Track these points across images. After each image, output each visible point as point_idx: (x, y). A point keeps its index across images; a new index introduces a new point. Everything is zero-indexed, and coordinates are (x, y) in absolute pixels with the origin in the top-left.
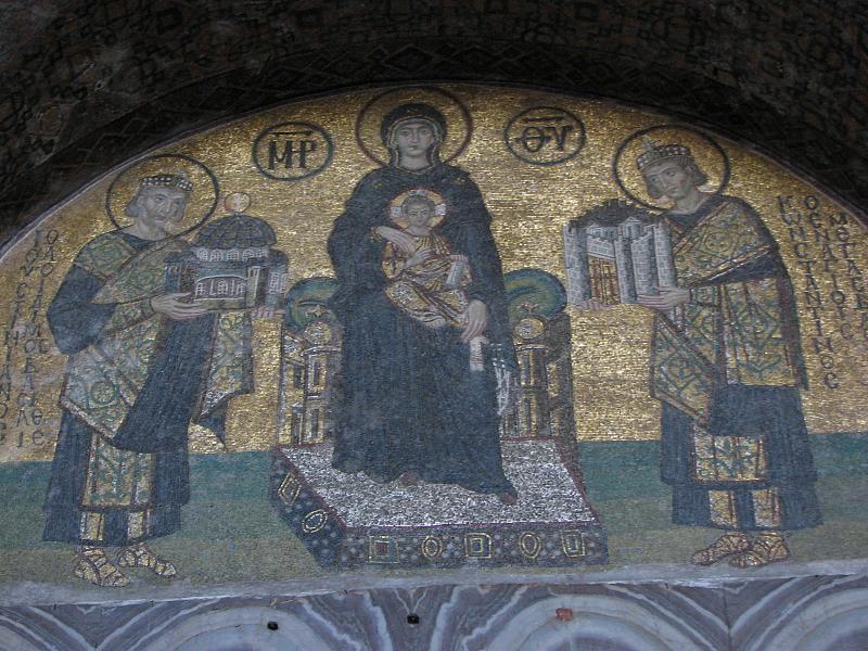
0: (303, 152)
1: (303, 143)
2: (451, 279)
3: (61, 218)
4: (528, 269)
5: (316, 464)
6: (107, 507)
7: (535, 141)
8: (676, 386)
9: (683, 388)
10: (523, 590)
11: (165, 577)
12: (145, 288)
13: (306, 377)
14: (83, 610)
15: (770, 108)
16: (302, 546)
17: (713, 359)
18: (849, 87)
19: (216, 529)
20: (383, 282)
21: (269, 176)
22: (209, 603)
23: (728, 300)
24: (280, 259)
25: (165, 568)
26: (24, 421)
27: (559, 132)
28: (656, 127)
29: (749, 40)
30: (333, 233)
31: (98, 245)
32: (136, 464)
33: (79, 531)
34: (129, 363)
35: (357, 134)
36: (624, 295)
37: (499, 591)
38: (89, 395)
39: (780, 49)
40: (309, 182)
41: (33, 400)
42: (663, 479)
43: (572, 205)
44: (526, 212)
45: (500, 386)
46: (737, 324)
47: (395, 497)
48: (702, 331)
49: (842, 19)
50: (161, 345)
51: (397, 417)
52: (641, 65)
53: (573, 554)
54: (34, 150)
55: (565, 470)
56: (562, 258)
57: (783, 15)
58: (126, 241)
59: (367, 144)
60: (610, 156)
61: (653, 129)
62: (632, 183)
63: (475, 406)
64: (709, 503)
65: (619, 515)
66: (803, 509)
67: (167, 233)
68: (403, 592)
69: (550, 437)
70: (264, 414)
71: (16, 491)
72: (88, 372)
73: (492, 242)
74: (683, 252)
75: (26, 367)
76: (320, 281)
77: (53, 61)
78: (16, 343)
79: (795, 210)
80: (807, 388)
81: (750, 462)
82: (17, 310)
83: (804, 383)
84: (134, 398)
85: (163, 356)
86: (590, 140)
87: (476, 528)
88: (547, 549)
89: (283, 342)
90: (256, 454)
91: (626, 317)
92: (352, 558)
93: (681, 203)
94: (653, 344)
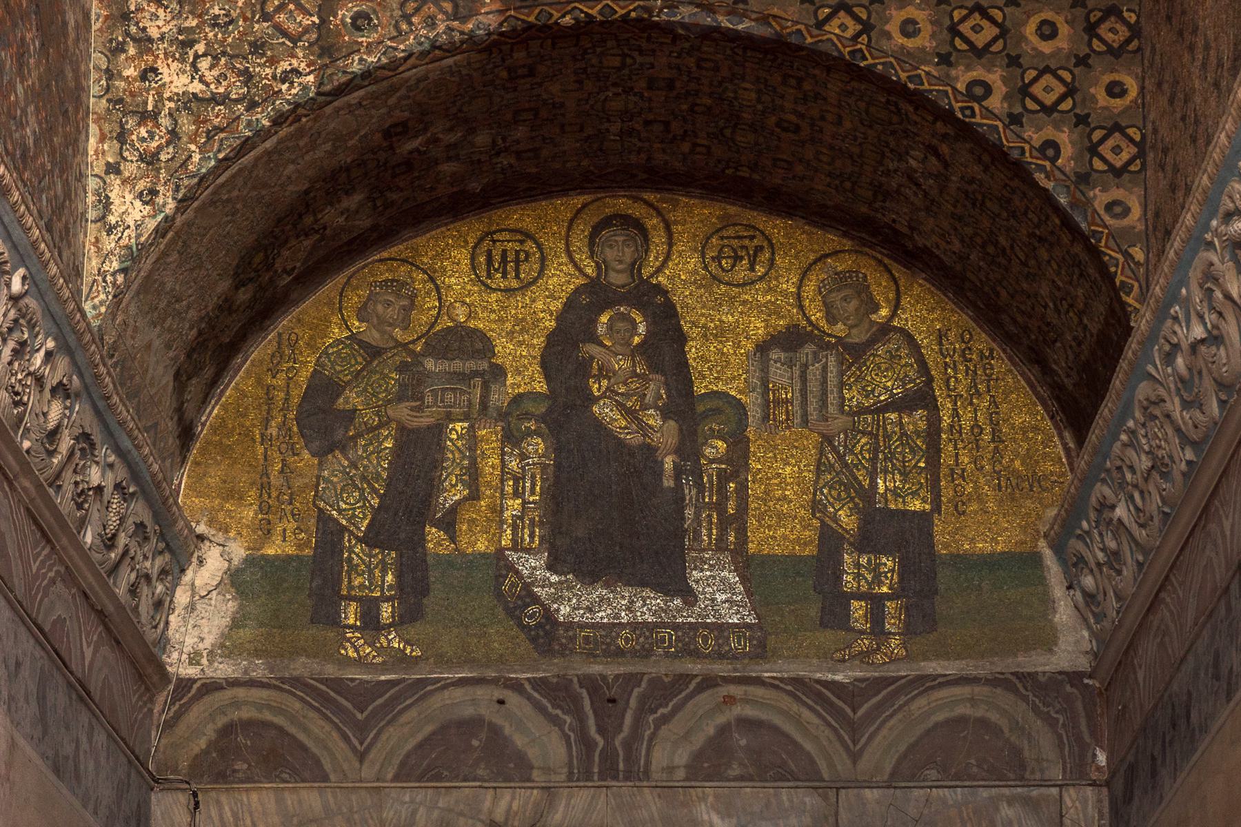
5: (532, 565)
13: (524, 488)
17: (866, 483)
26: (285, 519)
46: (890, 452)
50: (398, 450)
76: (533, 396)
89: (503, 454)
91: (796, 440)
94: (818, 468)
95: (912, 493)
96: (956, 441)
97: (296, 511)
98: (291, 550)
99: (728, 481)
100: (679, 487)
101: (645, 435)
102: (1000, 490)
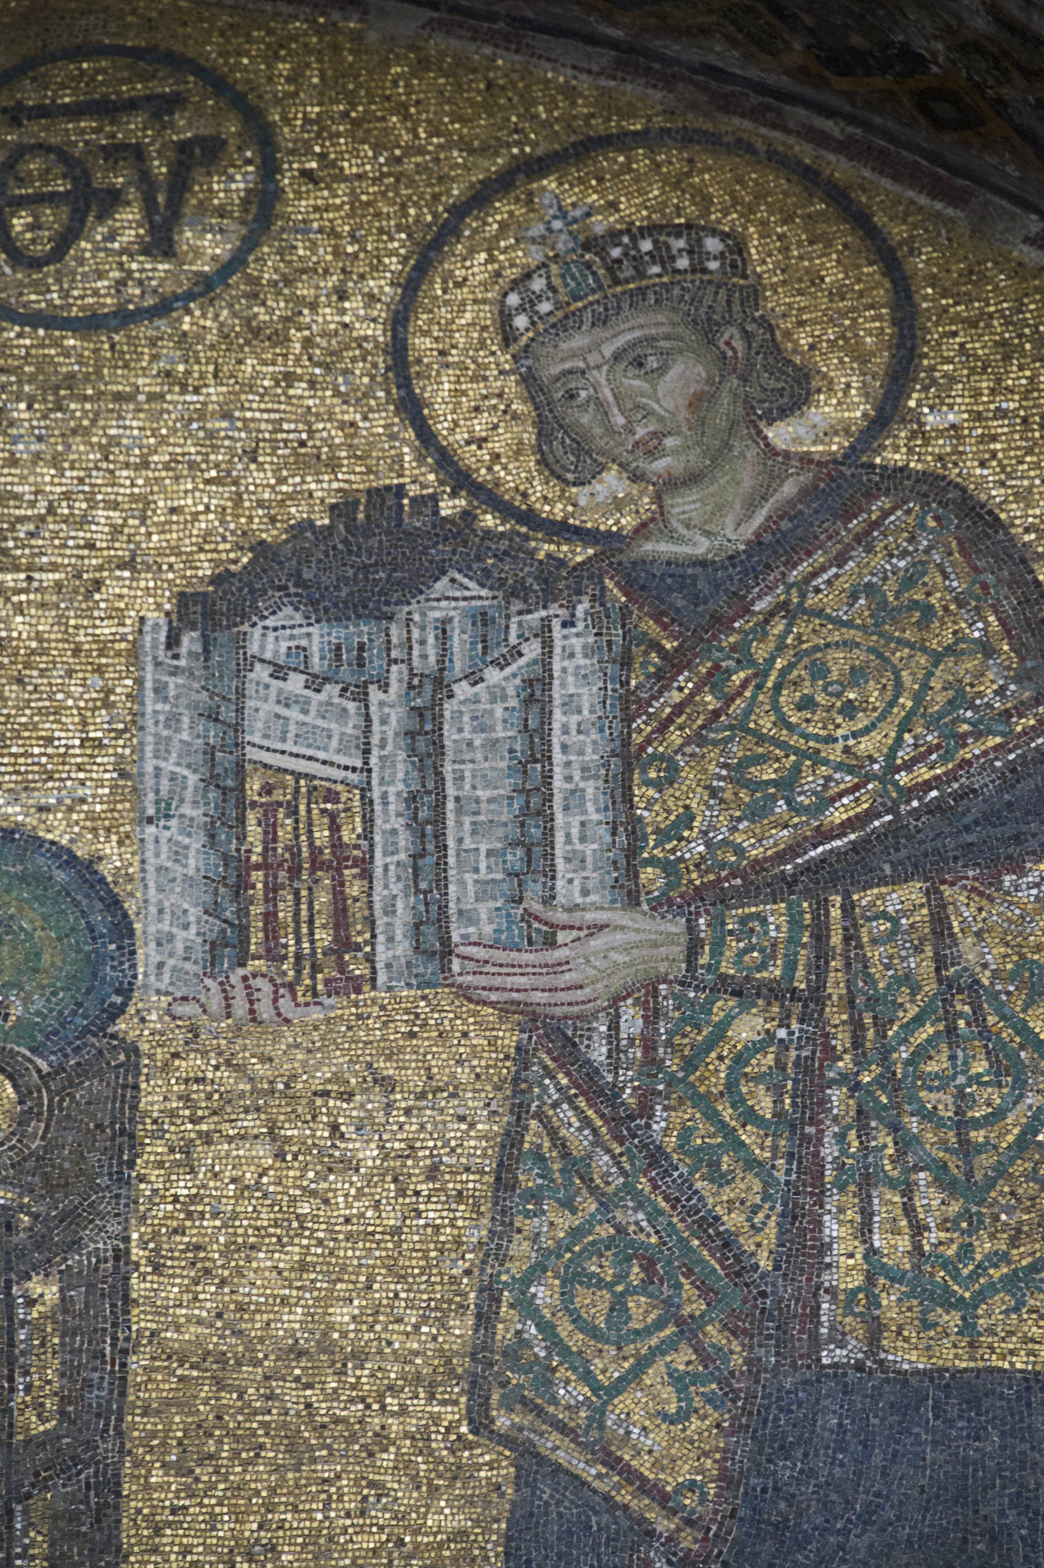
7: (48, 214)
8: (587, 1377)
9: (618, 1387)
27: (160, 169)
28: (606, 142)
48: (727, 1113)
60: (381, 285)
74: (675, 737)
95: (1011, 1282)
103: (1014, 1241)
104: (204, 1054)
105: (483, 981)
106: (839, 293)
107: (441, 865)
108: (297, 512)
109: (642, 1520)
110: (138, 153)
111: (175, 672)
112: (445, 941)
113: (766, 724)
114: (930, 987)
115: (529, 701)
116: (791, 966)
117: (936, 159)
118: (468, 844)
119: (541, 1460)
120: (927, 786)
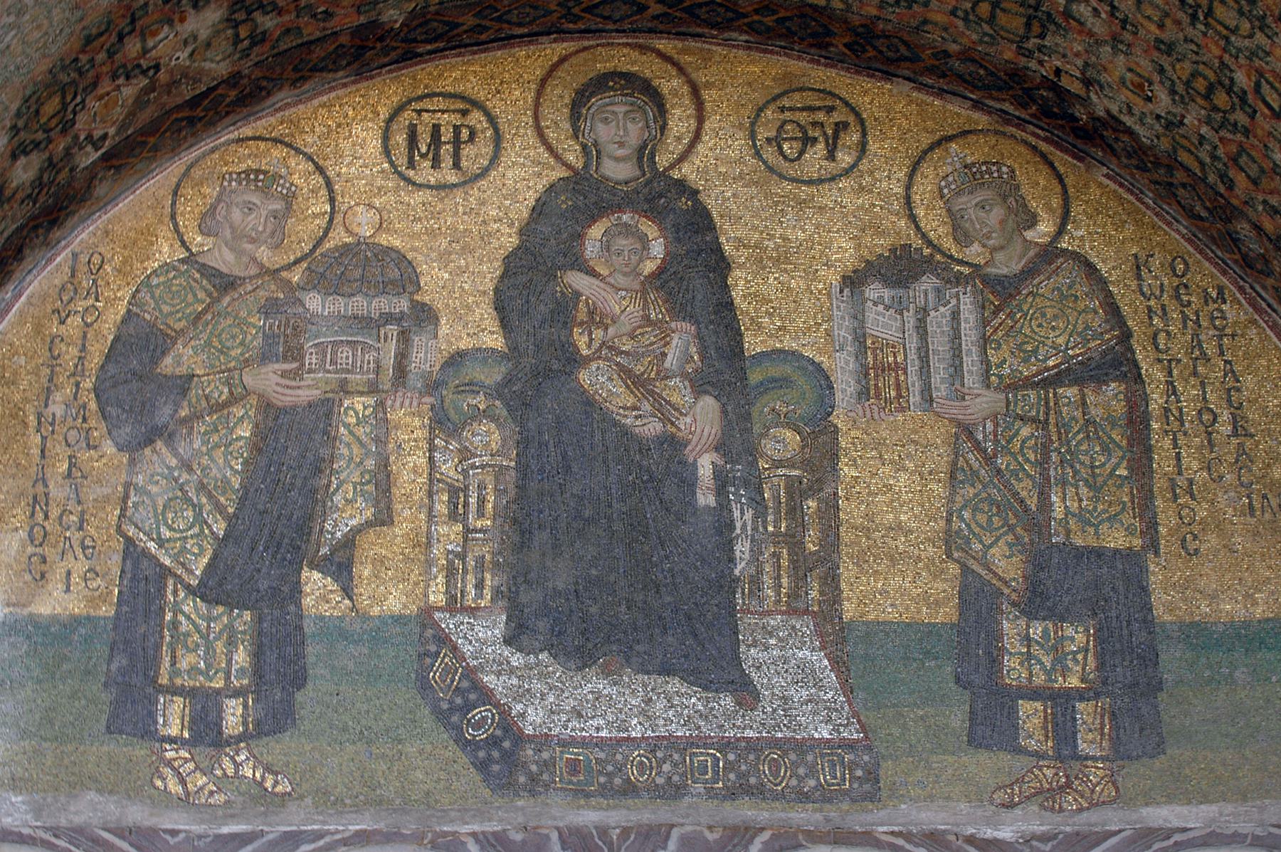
0: (457, 143)
1: (457, 129)
2: (671, 361)
3: (107, 233)
4: (781, 351)
6: (193, 689)
7: (795, 144)
8: (981, 542)
9: (991, 546)
10: (766, 835)
11: (273, 793)
12: (233, 353)
13: (466, 504)
14: (168, 837)
15: (1129, 132)
16: (465, 760)
17: (1033, 503)
18: (1239, 137)
19: (345, 729)
20: (574, 361)
21: (409, 181)
22: (338, 837)
23: (1057, 413)
24: (424, 316)
25: (276, 783)
26: (70, 555)
27: (830, 132)
29: (1108, 49)
30: (502, 277)
31: (162, 279)
32: (230, 628)
33: (156, 722)
34: (214, 471)
35: (536, 117)
36: (915, 398)
37: (731, 838)
38: (160, 518)
39: (1150, 69)
40: (466, 193)
41: (82, 521)
42: (958, 680)
43: (845, 253)
44: (782, 259)
45: (738, 531)
47: (592, 692)
48: (1020, 459)
49: (1237, 58)
50: (260, 443)
51: (594, 572)
52: (954, 48)
53: (833, 785)
54: (81, 148)
55: (826, 662)
56: (828, 333)
57: (1157, 32)
58: (202, 274)
59: (551, 135)
61: (965, 133)
62: (935, 225)
63: (703, 560)
64: (1018, 718)
65: (896, 731)
66: (1142, 730)
67: (262, 266)
68: (603, 831)
69: (806, 612)
70: (407, 559)
71: (65, 658)
72: (157, 482)
73: (730, 305)
74: (1000, 334)
75: (70, 469)
77: (121, 38)
78: (53, 432)
79: (1156, 278)
80: (1157, 553)
81: (1075, 660)
82: (51, 380)
83: (1154, 546)
84: (223, 525)
85: (263, 461)
86: (873, 146)
87: (703, 742)
88: (798, 776)
89: (432, 448)
90: (399, 619)
91: (916, 432)
92: (533, 779)
93: (999, 256)
94: (952, 476)
95: (1109, 519)
96: (1174, 435)
97: (88, 542)
98: (76, 606)
99: (804, 495)
100: (723, 505)
101: (666, 420)
102: (1252, 515)
103: (1110, 506)
104: (858, 429)
105: (943, 410)
106: (1045, 189)
107: (929, 372)
108: (879, 251)
109: (999, 589)
110: (822, 125)
111: (843, 302)
112: (931, 397)
113: (1027, 331)
114: (1082, 422)
115: (953, 319)
116: (1038, 412)
117: (1074, 146)
118: (937, 365)
119: (968, 568)
120: (1078, 355)
